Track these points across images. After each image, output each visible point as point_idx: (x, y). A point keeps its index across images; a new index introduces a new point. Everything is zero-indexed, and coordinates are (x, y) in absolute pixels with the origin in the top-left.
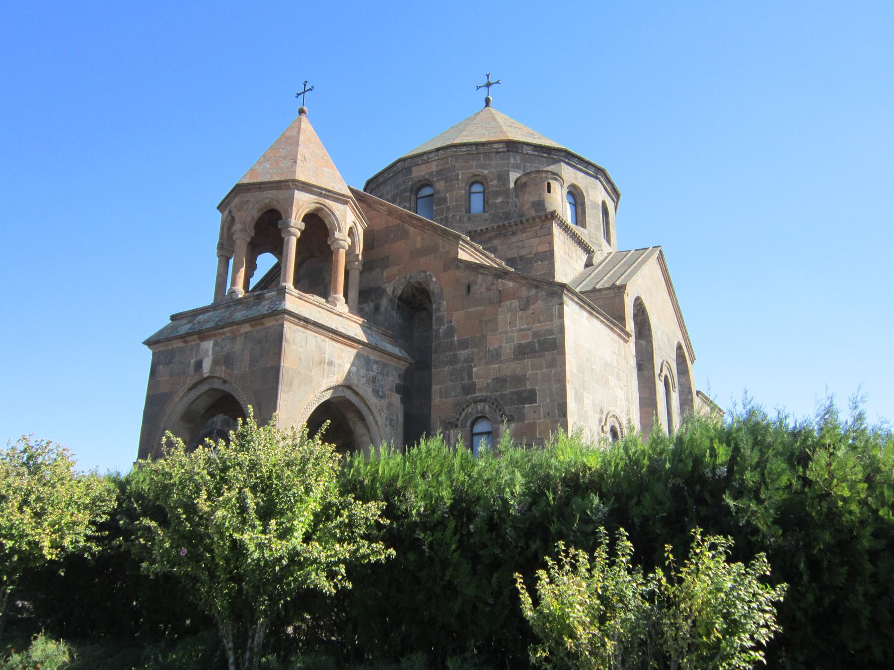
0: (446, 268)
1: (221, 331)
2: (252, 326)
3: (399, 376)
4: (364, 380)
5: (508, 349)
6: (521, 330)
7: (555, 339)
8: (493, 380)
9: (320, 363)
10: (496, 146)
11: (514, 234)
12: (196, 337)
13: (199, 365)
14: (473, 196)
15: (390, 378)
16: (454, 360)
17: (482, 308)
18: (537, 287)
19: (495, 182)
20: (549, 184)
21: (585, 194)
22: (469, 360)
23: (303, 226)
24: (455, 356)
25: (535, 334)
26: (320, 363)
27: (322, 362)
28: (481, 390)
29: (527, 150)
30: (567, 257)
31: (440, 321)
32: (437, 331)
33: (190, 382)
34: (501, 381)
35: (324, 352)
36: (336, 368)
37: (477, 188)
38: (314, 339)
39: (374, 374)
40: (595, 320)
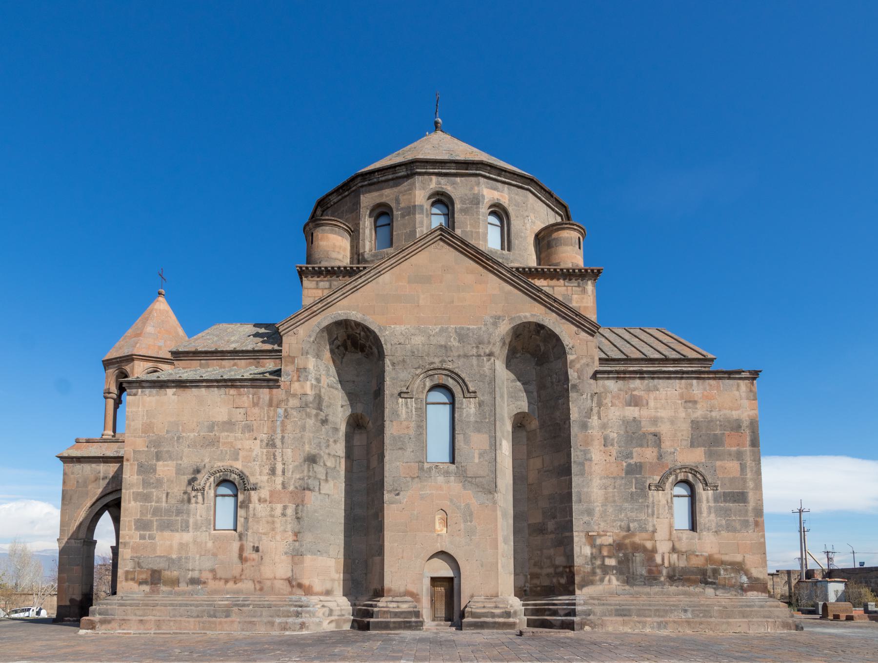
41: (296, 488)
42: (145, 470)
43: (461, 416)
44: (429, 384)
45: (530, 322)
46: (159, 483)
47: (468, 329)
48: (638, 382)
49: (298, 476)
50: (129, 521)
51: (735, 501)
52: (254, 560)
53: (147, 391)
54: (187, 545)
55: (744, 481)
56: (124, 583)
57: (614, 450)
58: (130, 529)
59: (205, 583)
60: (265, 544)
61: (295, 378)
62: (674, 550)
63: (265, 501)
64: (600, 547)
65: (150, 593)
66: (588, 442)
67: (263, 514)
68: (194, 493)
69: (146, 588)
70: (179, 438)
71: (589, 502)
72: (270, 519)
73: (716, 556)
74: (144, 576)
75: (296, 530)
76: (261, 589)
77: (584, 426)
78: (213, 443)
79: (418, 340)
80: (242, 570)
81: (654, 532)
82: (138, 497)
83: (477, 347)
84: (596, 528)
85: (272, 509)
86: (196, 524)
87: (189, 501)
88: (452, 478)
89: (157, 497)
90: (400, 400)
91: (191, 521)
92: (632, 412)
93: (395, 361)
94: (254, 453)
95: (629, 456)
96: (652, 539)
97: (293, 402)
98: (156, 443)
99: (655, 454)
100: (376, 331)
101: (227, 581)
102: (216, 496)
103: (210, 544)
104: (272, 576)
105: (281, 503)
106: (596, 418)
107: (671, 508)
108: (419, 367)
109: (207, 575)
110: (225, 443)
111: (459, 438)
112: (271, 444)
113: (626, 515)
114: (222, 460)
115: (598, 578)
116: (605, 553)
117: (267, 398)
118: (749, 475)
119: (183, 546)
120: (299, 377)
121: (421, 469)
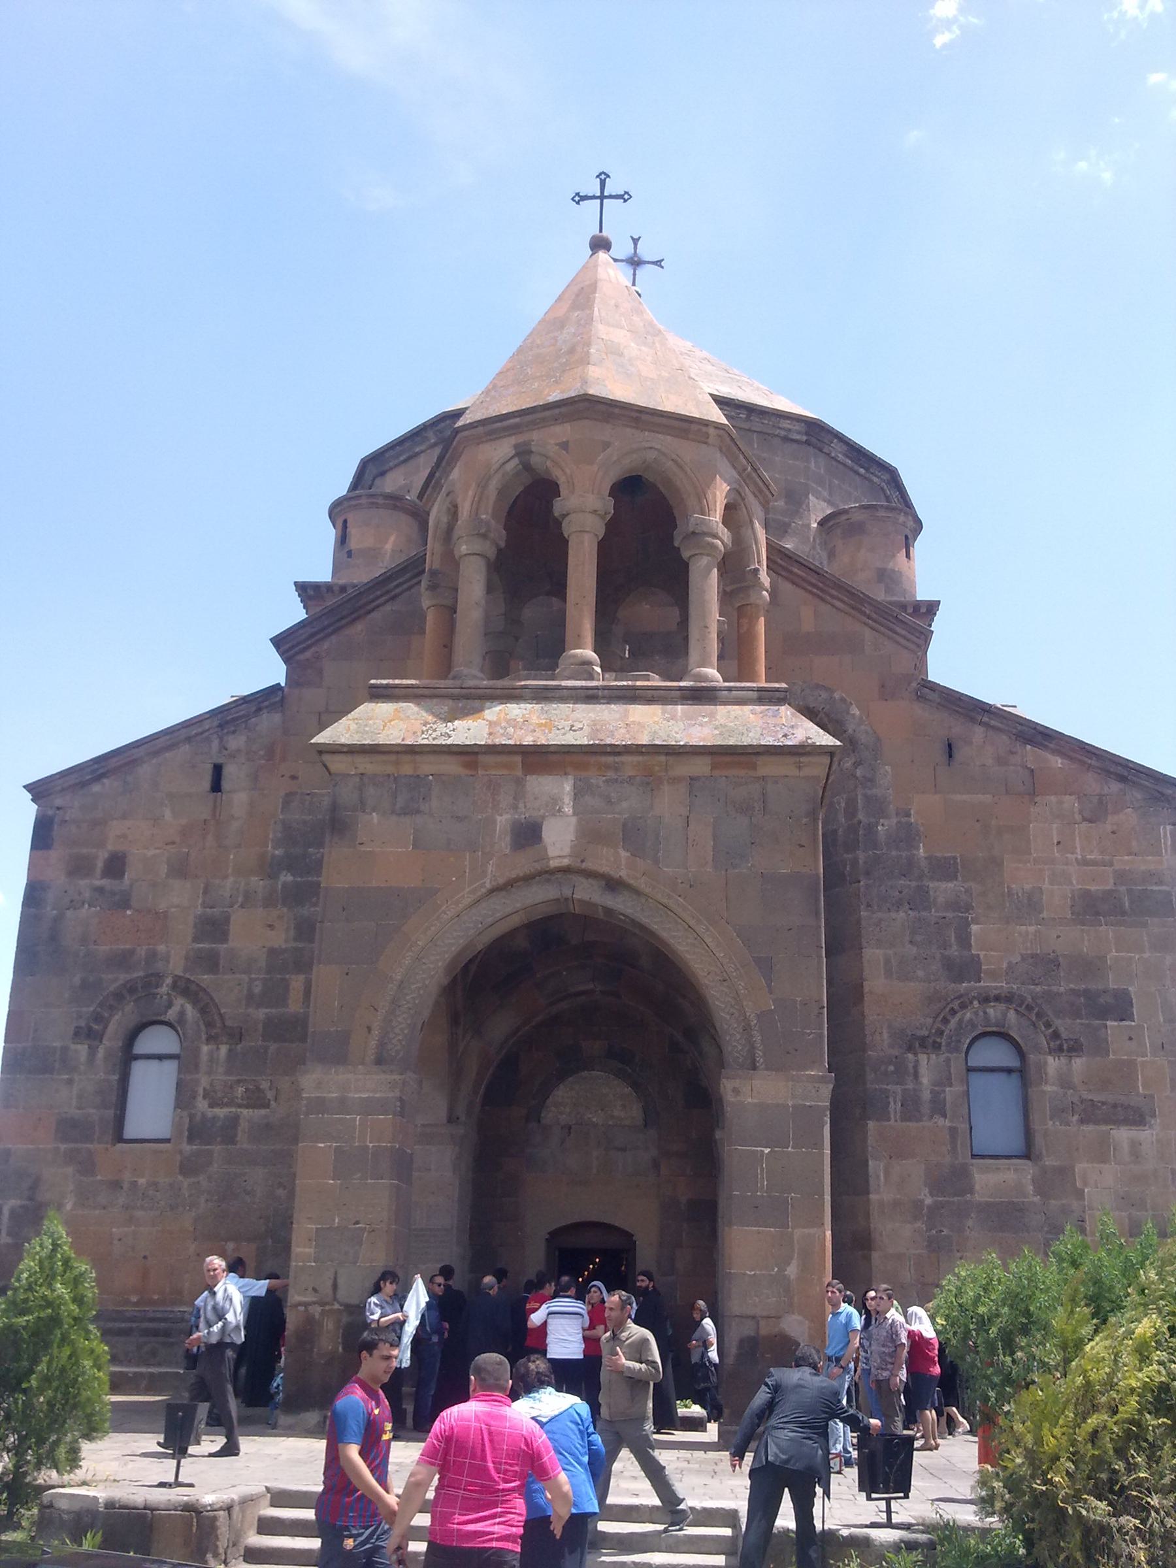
0: (886, 691)
1: (610, 759)
2: (714, 767)
5: (1057, 898)
6: (1086, 863)
7: (1169, 894)
8: (1023, 958)
10: (786, 424)
12: (518, 759)
13: (528, 834)
16: (920, 900)
17: (987, 798)
18: (1122, 779)
22: (960, 906)
24: (923, 892)
25: (1121, 877)
28: (993, 975)
29: (837, 450)
31: (878, 808)
32: (871, 829)
33: (493, 873)
34: (1048, 964)
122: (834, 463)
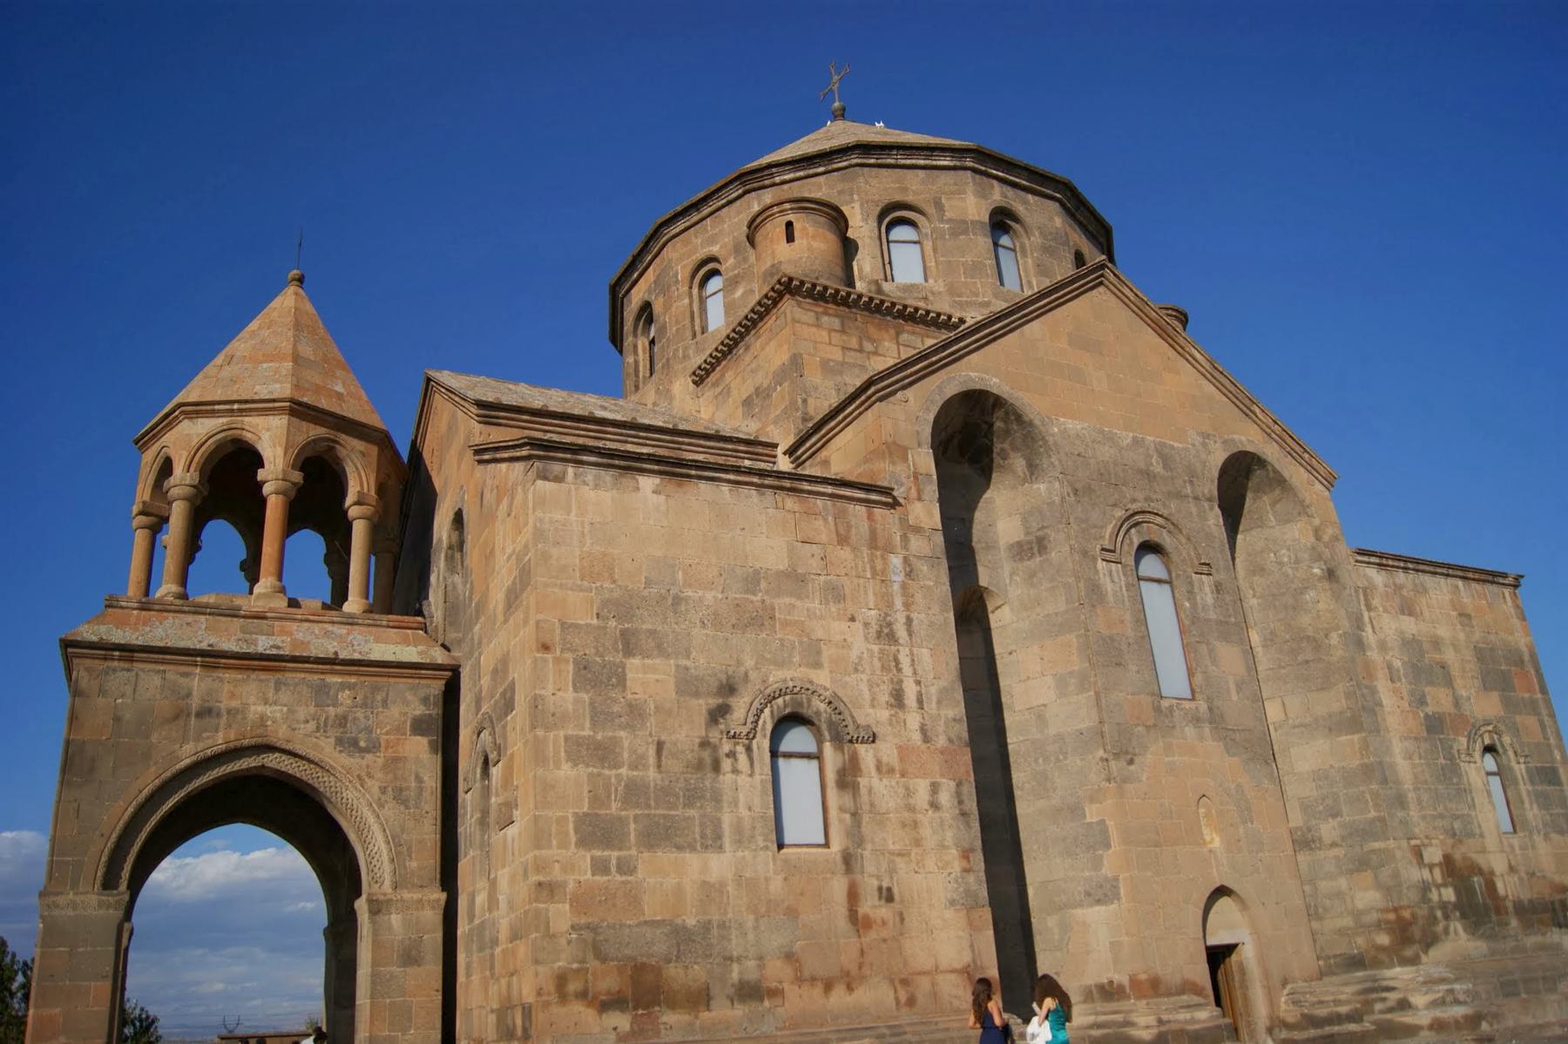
3: (425, 701)
4: (312, 726)
9: (177, 717)
11: (747, 348)
14: (710, 302)
15: (395, 711)
19: (731, 261)
20: (789, 225)
21: (931, 210)
23: (192, 477)
26: (177, 717)
27: (179, 715)
30: (852, 357)
35: (189, 695)
36: (224, 720)
37: (715, 284)
38: (157, 680)
39: (340, 710)
40: (703, 485)
41: (950, 740)
42: (597, 677)
43: (1194, 605)
44: (1136, 543)
45: (1246, 453)
46: (636, 712)
47: (1173, 447)
48: (1401, 577)
49: (951, 714)
50: (561, 821)
51: (1550, 783)
52: (884, 923)
53: (590, 474)
54: (722, 884)
55: (1549, 746)
56: (557, 1010)
57: (1404, 687)
58: (563, 845)
59: (775, 993)
60: (908, 880)
61: (914, 493)
62: (1512, 869)
63: (891, 771)
64: (1431, 867)
65: (633, 1033)
66: (1371, 675)
67: (892, 804)
68: (726, 747)
69: (621, 1021)
70: (677, 601)
71: (1397, 782)
72: (906, 815)
73: (1557, 879)
74: (609, 982)
75: (966, 846)
76: (911, 1002)
77: (1360, 645)
78: (761, 619)
79: (1106, 453)
80: (862, 952)
81: (1482, 835)
82: (580, 750)
83: (1191, 482)
84: (1417, 830)
85: (909, 792)
86: (738, 829)
87: (716, 767)
88: (1207, 730)
89: (633, 751)
90: (1101, 565)
91: (727, 820)
92: (1409, 625)
93: (1079, 486)
94: (854, 654)
95: (1422, 702)
96: (1484, 851)
97: (917, 544)
98: (623, 607)
99: (1450, 699)
100: (1037, 422)
101: (828, 987)
102: (774, 754)
103: (777, 886)
104: (929, 966)
105: (924, 776)
106: (1369, 629)
107: (1489, 793)
108: (1115, 505)
109: (777, 972)
110: (786, 624)
111: (1203, 649)
112: (886, 634)
113: (1446, 808)
114: (781, 664)
115: (1440, 928)
116: (1437, 872)
117: (864, 527)
118: (1552, 741)
119: (711, 892)
120: (919, 492)
121: (1158, 709)
122: (786, 187)
